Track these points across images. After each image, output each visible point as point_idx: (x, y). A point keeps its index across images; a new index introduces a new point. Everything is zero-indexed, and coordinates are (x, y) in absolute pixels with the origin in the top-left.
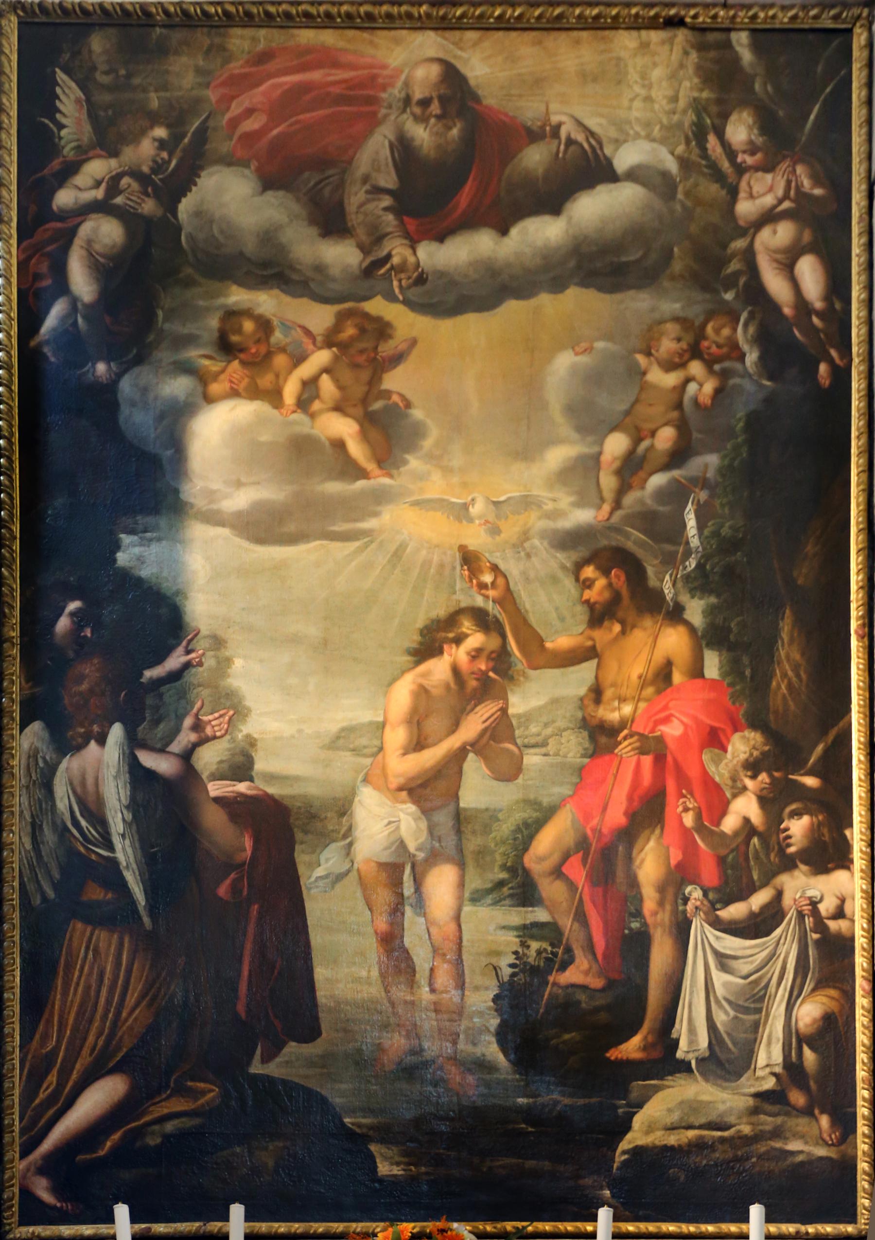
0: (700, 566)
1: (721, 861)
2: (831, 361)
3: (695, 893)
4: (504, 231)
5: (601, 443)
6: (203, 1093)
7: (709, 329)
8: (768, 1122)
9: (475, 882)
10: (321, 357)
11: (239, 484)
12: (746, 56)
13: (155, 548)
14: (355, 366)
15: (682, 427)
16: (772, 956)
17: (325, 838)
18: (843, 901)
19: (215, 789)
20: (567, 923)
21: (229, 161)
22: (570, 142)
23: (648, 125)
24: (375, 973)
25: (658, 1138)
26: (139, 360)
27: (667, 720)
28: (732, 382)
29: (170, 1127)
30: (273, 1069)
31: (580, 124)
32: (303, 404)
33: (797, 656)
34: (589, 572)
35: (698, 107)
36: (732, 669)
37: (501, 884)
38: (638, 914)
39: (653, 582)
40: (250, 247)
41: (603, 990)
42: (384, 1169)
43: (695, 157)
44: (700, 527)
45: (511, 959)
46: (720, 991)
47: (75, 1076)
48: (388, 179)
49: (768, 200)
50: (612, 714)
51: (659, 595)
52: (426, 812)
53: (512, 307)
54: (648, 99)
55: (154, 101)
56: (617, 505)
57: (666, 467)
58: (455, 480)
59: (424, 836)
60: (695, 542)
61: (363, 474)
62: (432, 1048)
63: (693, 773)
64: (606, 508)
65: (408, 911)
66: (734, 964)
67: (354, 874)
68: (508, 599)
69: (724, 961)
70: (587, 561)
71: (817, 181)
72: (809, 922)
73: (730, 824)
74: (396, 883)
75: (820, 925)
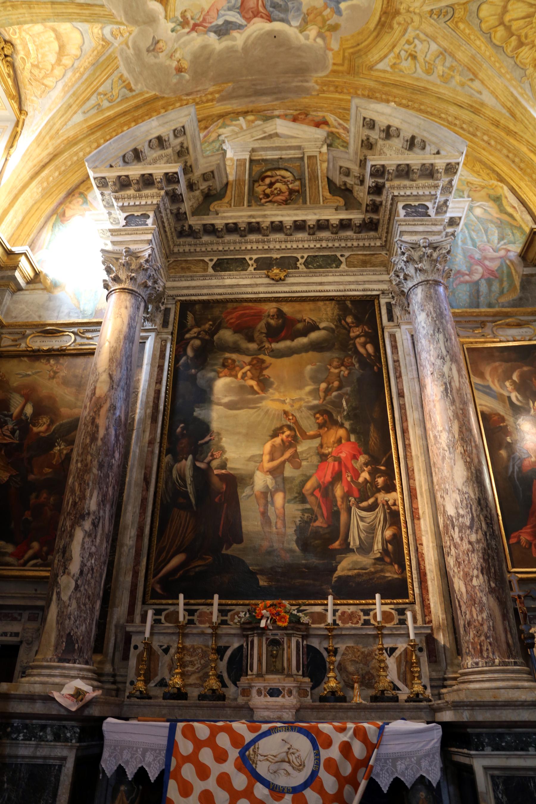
0: (347, 414)
1: (359, 490)
2: (377, 366)
3: (352, 499)
4: (293, 340)
5: (319, 385)
6: (208, 559)
7: (346, 360)
8: (379, 567)
9: (288, 497)
10: (248, 368)
11: (226, 396)
12: (350, 305)
13: (204, 411)
14: (256, 369)
15: (340, 381)
16: (376, 517)
17: (246, 485)
18: (395, 501)
19: (216, 472)
20: (316, 508)
21: (226, 328)
22: (308, 322)
23: (327, 319)
24: (259, 523)
26: (202, 369)
27: (341, 452)
28: (353, 371)
29: (197, 569)
30: (229, 552)
31: (311, 319)
32: (243, 378)
33: (376, 435)
34: (318, 415)
35: (338, 315)
36: (358, 439)
37: (296, 497)
38: (336, 505)
39: (335, 417)
41: (327, 528)
42: (262, 583)
43: (339, 324)
44: (347, 404)
45: (300, 519)
46: (361, 527)
47: (171, 553)
48: (264, 331)
49: (358, 333)
50: (326, 451)
51: (337, 421)
52: (274, 478)
53: (296, 356)
54: (327, 314)
55: (209, 317)
56: (324, 399)
57: (337, 390)
58: (282, 394)
59: (274, 484)
60: (346, 408)
61: (258, 393)
62: (276, 545)
63: (349, 466)
64: (322, 400)
65: (269, 506)
66: (365, 519)
67: (254, 495)
68: (296, 422)
69: (362, 519)
70: (317, 413)
71: (369, 329)
72: (386, 507)
73: (361, 480)
74: (266, 498)
75: (389, 508)
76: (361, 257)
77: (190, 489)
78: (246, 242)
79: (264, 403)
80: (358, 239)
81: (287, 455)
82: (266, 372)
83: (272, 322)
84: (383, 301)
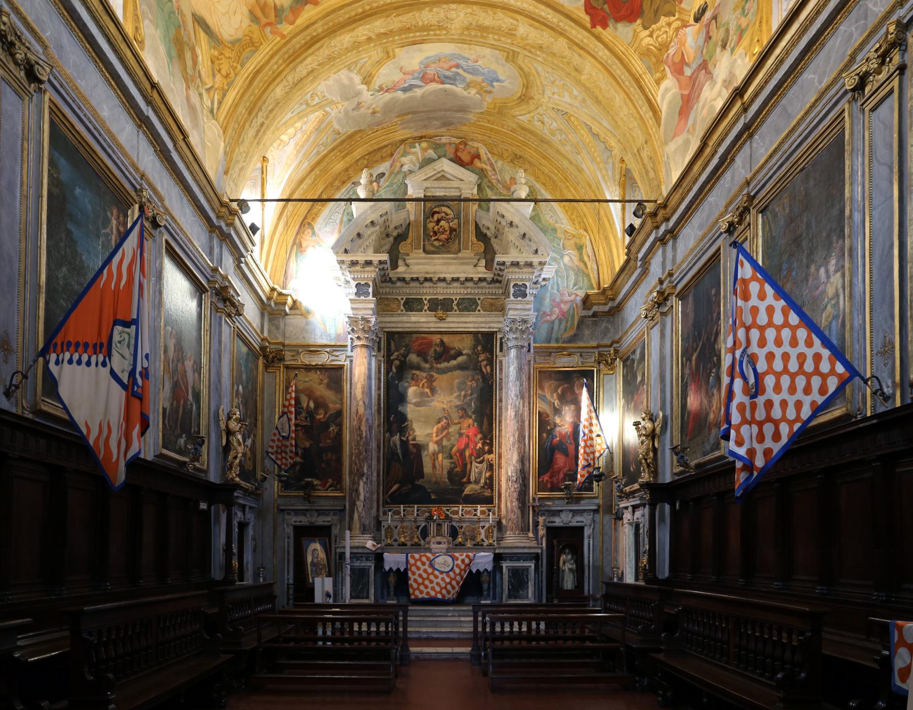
9: (444, 456)
10: (425, 380)
19: (411, 442)
30: (418, 483)
32: (422, 387)
36: (478, 425)
40: (416, 364)
48: (433, 355)
68: (449, 415)
73: (478, 447)
76: (489, 300)
77: (399, 451)
78: (423, 287)
80: (489, 288)
81: (444, 433)
82: (434, 384)
84: (499, 336)
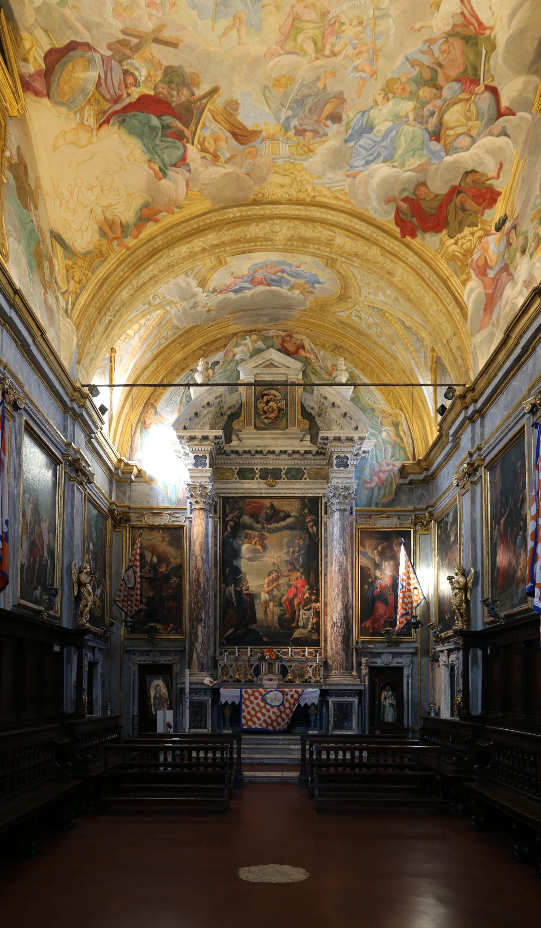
15: (299, 547)
25: (297, 636)
30: (252, 627)
36: (305, 577)
48: (264, 517)
53: (279, 533)
68: (279, 568)
69: (305, 614)
73: (305, 597)
76: (315, 470)
77: (234, 600)
79: (264, 559)
81: (275, 584)
82: (265, 542)
83: (268, 511)
84: (324, 501)
